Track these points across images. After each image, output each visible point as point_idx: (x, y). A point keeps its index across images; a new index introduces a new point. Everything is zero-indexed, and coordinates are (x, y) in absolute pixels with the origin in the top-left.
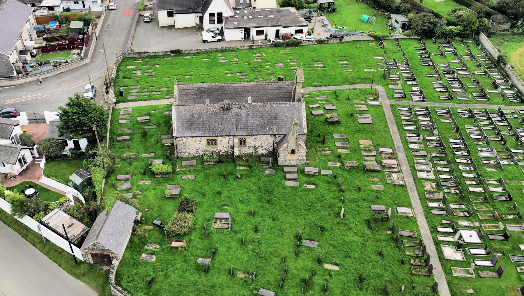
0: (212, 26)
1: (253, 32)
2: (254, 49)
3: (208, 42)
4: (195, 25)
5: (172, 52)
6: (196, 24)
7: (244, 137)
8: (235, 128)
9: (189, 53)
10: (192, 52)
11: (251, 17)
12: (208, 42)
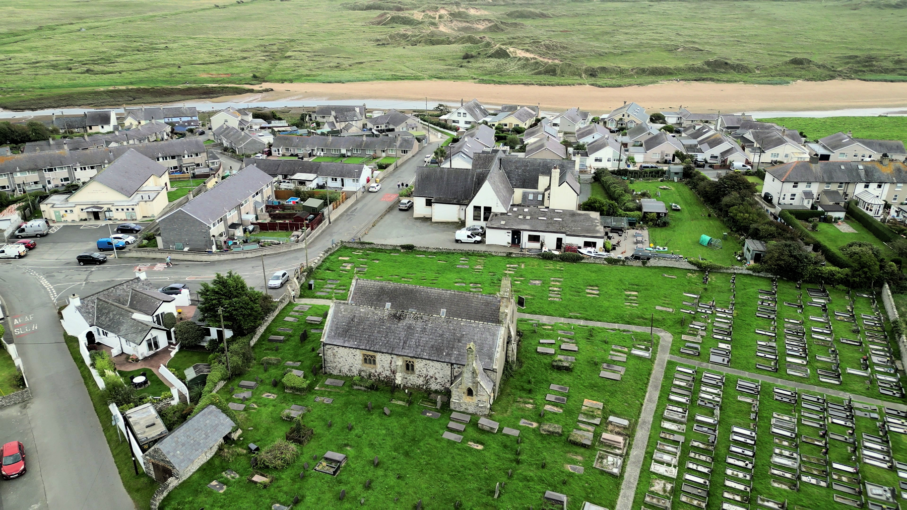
4: (457, 220)
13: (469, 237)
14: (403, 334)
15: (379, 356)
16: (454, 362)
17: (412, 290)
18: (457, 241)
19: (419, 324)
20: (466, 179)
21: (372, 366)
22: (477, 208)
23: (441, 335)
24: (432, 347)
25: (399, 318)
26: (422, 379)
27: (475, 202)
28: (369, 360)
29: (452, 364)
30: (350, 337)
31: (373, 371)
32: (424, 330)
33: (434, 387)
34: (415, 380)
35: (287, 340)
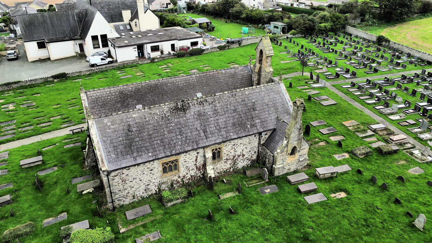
0: (97, 50)
1: (148, 48)
2: (156, 62)
3: (97, 66)
4: (75, 55)
5: (55, 77)
6: (77, 53)
7: (217, 146)
8: (202, 134)
9: (78, 76)
10: (82, 74)
11: (140, 36)
12: (97, 66)
13: (102, 59)
14: (197, 124)
15: (182, 158)
16: (261, 130)
17: (156, 85)
18: (93, 66)
19: (208, 108)
20: (68, 19)
21: (174, 172)
22: (95, 38)
23: (235, 111)
24: (234, 124)
25: (184, 109)
26: (230, 162)
27: (92, 32)
28: (170, 167)
29: (260, 134)
30: (139, 150)
31: (176, 178)
32: (216, 112)
33: (241, 164)
34: (223, 166)
35: (17, 197)
